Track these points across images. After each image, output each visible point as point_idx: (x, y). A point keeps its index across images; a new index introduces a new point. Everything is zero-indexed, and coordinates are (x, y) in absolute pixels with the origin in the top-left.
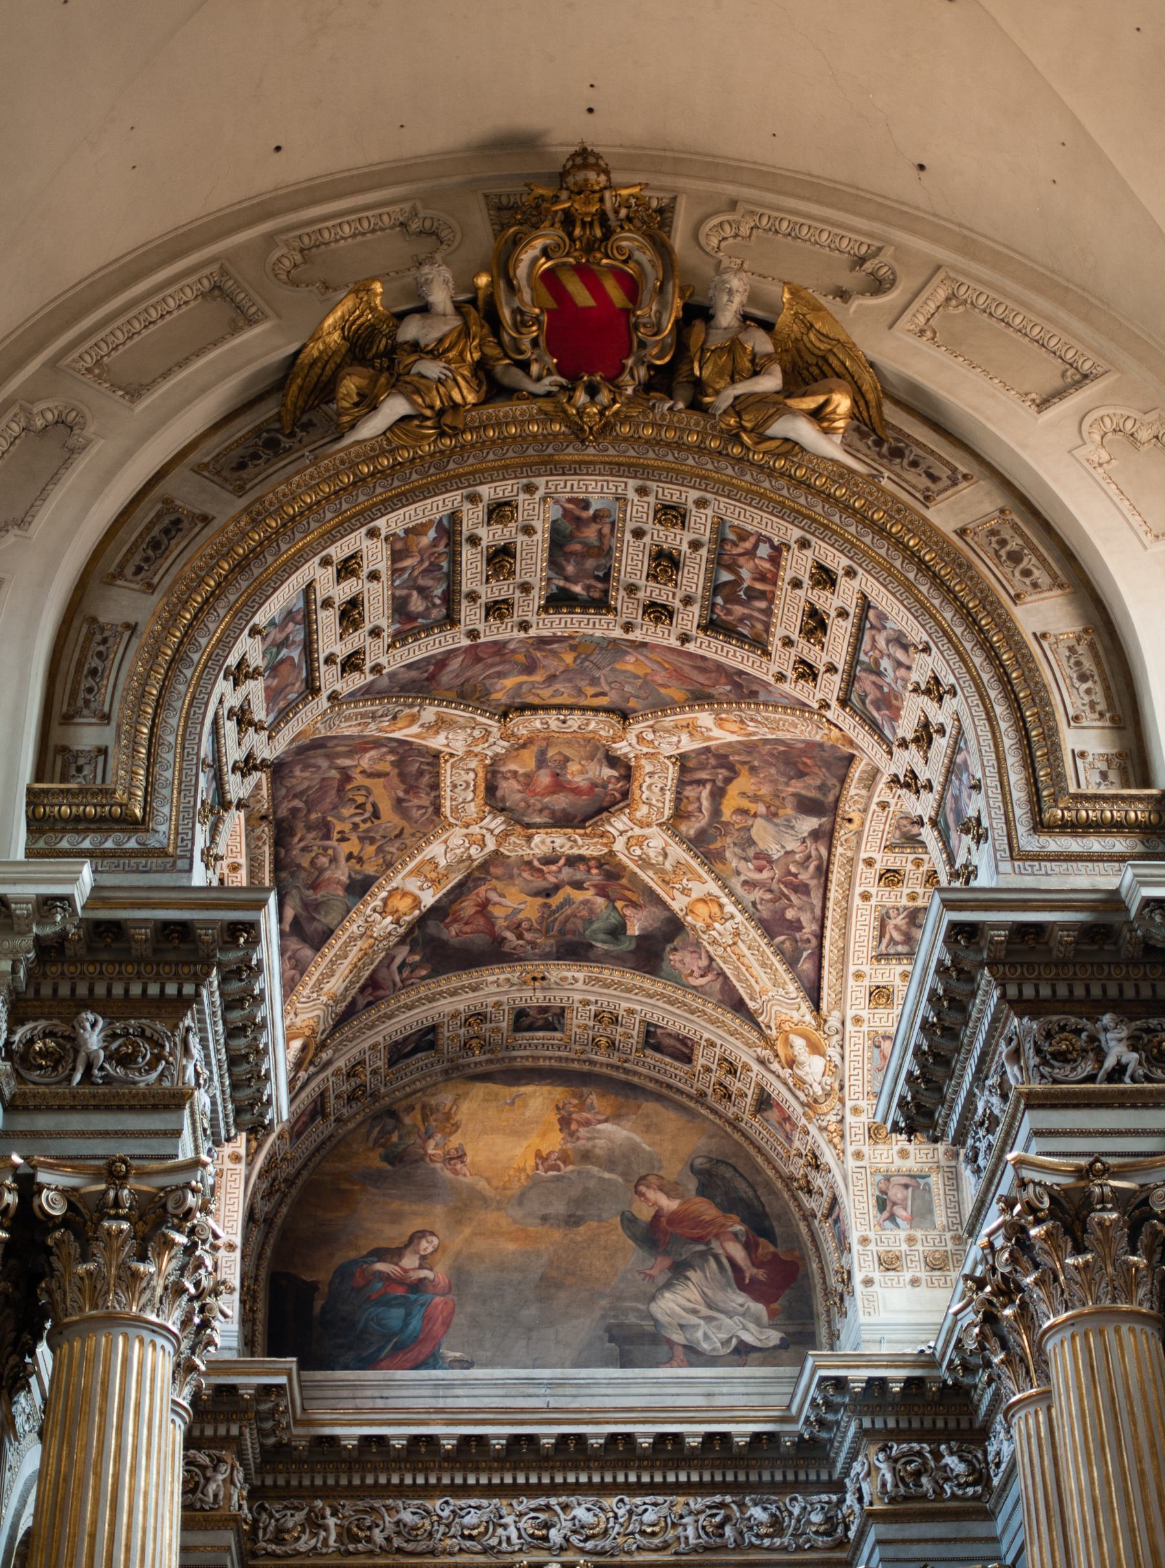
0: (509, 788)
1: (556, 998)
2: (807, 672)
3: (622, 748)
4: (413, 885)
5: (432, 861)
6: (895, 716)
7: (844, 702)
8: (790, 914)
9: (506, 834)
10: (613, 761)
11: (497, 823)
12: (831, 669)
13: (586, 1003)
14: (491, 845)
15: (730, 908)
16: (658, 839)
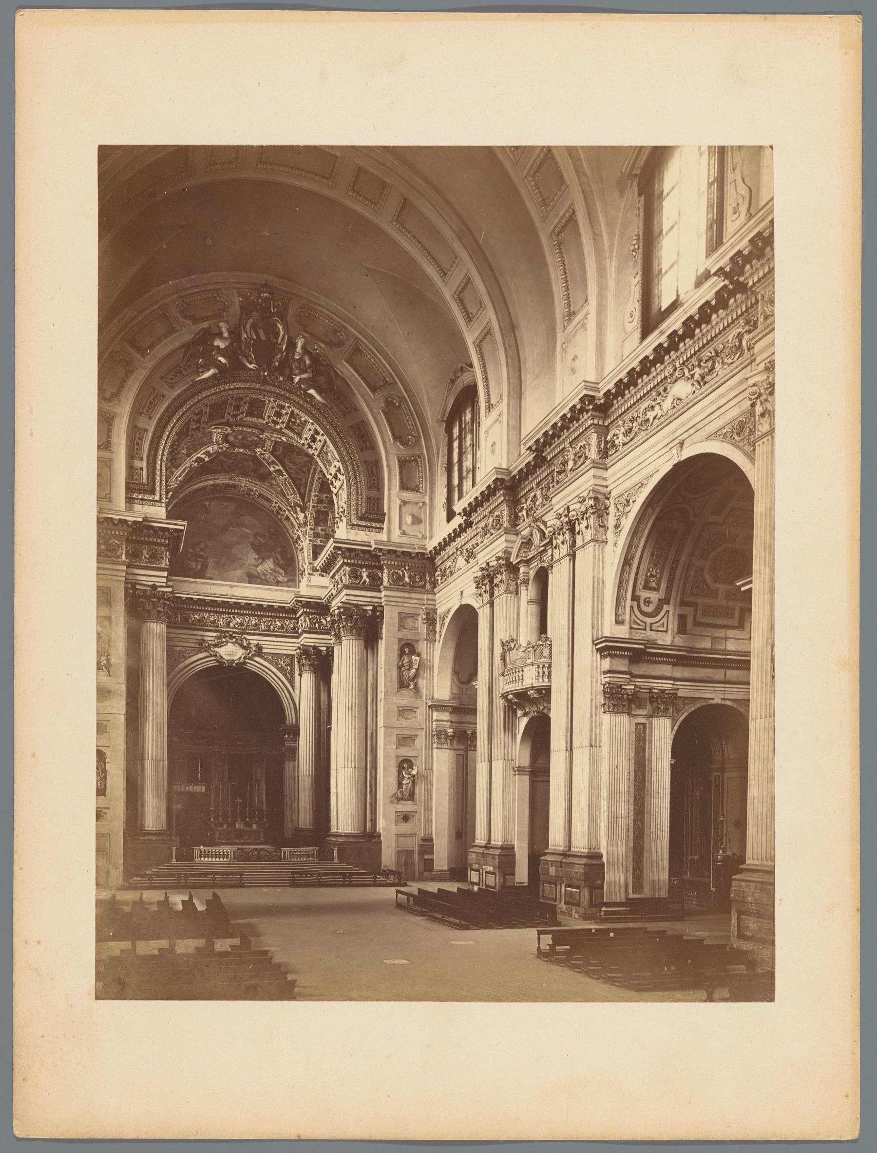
0: (231, 439)
1: (237, 483)
2: (311, 447)
3: (262, 436)
4: (203, 456)
5: (209, 452)
6: (330, 465)
7: (318, 456)
8: (300, 477)
9: (227, 448)
10: (259, 437)
11: (227, 445)
12: (316, 449)
13: (245, 486)
14: (224, 449)
15: (285, 473)
16: (268, 455)
